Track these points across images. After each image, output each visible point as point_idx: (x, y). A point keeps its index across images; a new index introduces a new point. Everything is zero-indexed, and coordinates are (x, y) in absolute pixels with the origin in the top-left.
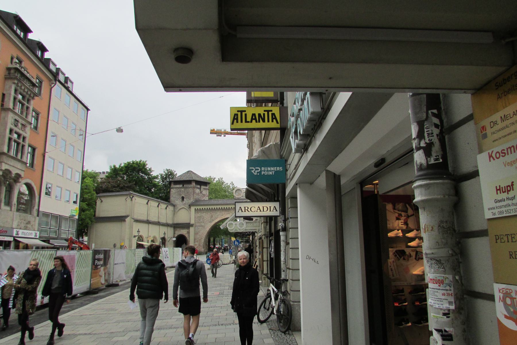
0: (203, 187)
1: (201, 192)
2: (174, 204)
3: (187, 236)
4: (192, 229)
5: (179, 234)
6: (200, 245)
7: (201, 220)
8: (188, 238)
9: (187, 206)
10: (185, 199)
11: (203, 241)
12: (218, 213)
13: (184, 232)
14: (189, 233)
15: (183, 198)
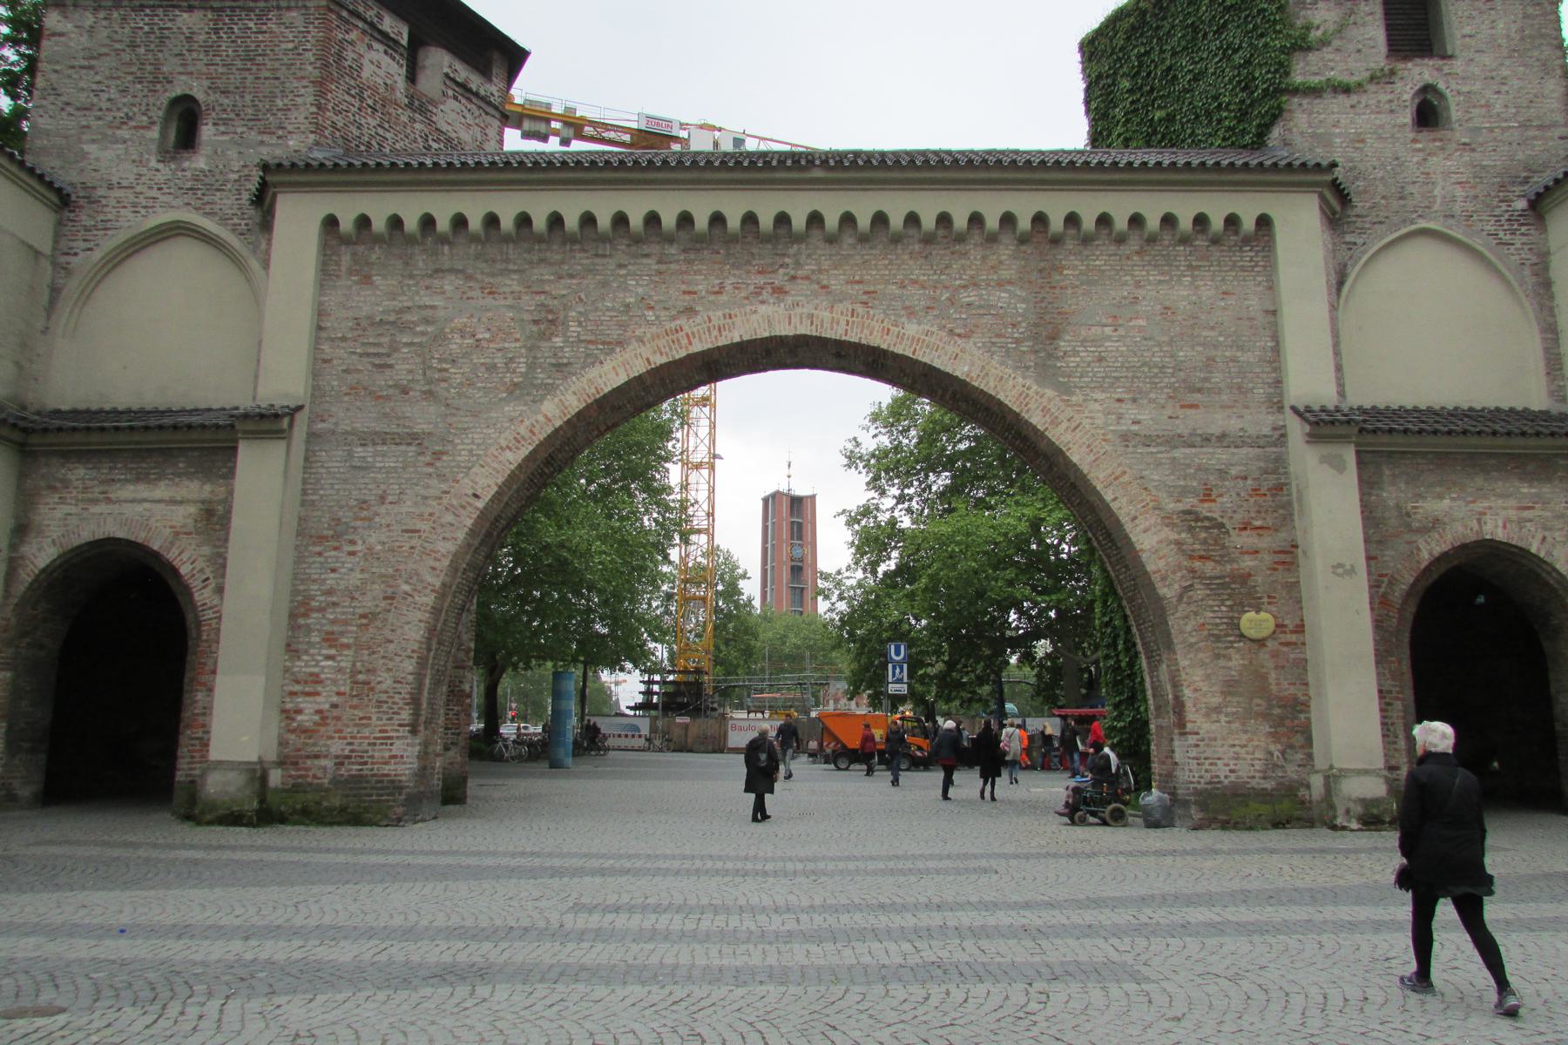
0: (439, 62)
1: (420, 106)
2: (66, 177)
3: (188, 560)
4: (260, 474)
5: (88, 533)
6: (362, 687)
7: (404, 367)
8: (203, 596)
9: (237, 202)
10: (207, 132)
11: (411, 627)
12: (635, 281)
13: (147, 510)
14: (215, 520)
15: (186, 121)
